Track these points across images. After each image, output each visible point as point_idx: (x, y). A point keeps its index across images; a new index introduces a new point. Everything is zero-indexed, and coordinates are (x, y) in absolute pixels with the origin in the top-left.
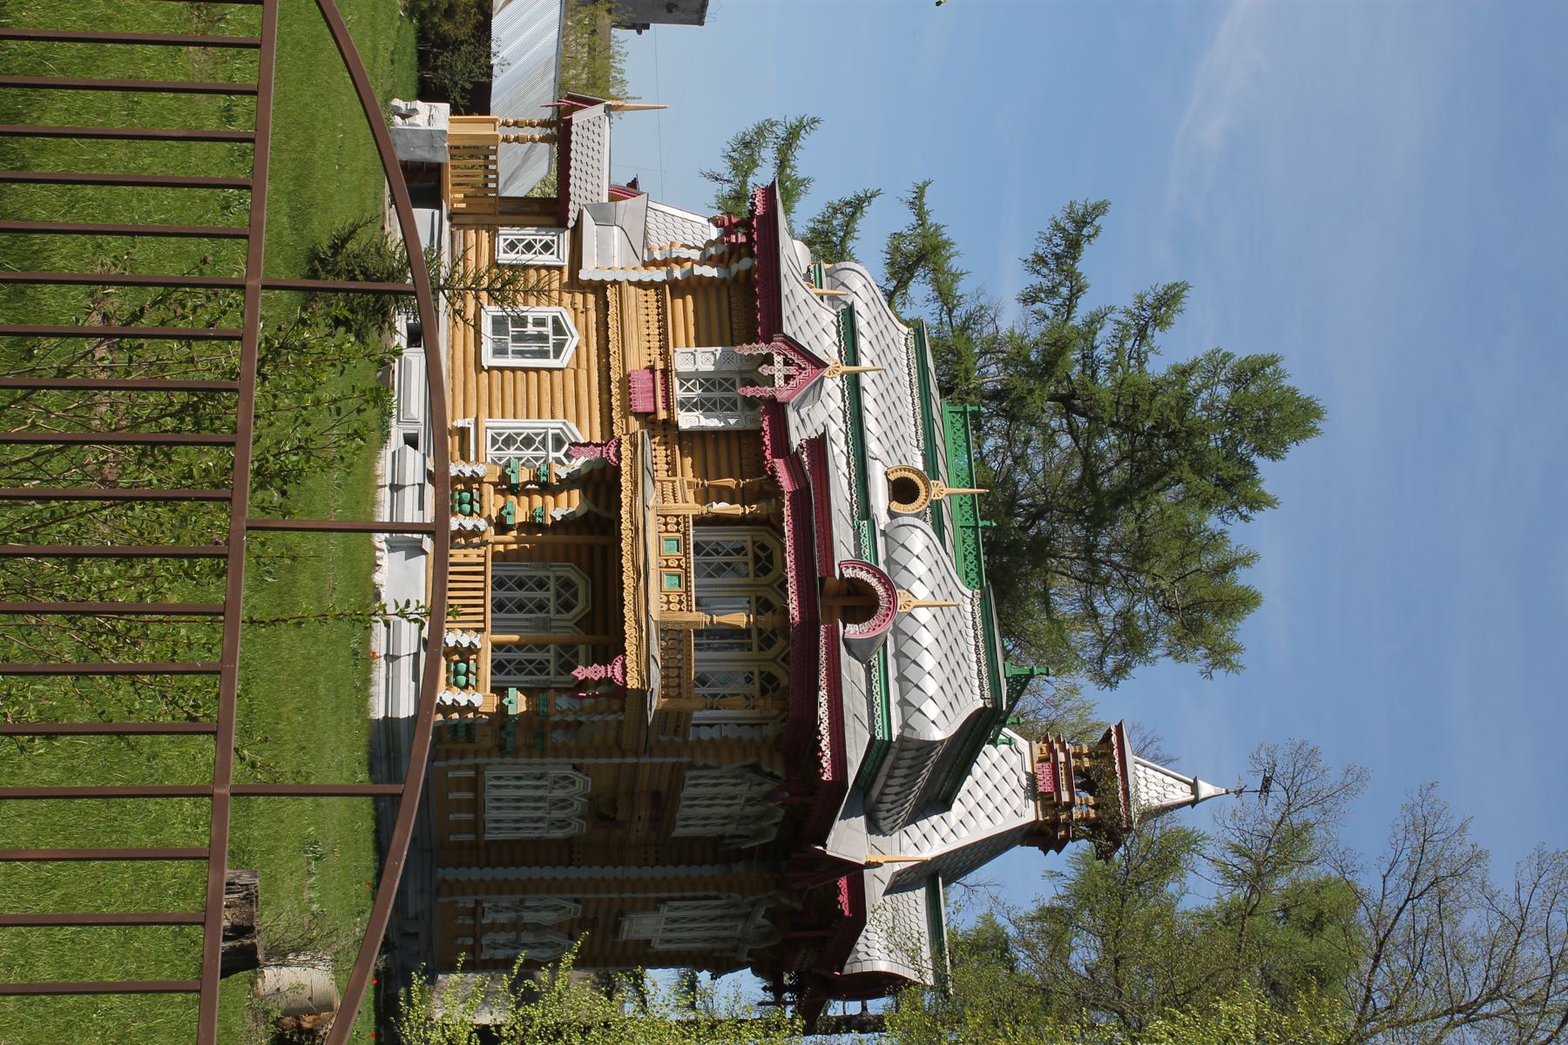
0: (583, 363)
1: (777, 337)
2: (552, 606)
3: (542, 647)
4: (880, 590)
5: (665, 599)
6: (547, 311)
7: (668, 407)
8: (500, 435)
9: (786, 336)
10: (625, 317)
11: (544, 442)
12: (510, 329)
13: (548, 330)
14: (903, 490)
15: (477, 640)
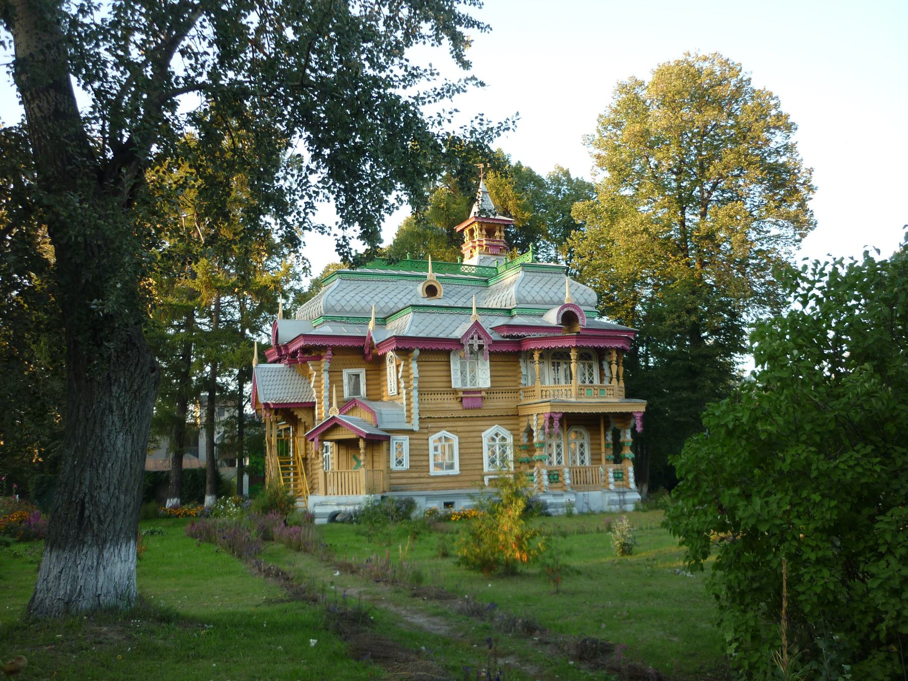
0: (455, 429)
1: (463, 342)
7: (480, 391)
13: (439, 445)
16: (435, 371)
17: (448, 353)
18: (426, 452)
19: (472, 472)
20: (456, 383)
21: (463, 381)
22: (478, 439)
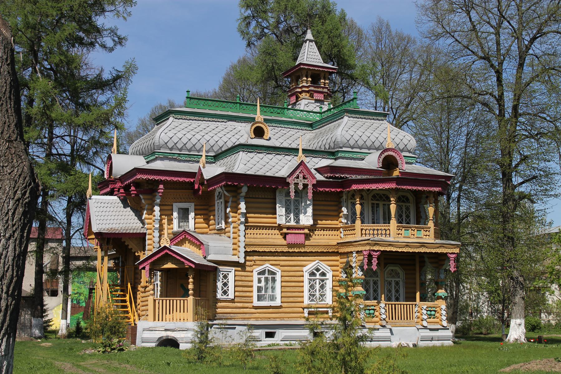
1: (289, 180)
2: (375, 279)
3: (390, 283)
6: (255, 277)
9: (288, 176)
10: (266, 243)
13: (263, 278)
17: (274, 191)
19: (293, 305)
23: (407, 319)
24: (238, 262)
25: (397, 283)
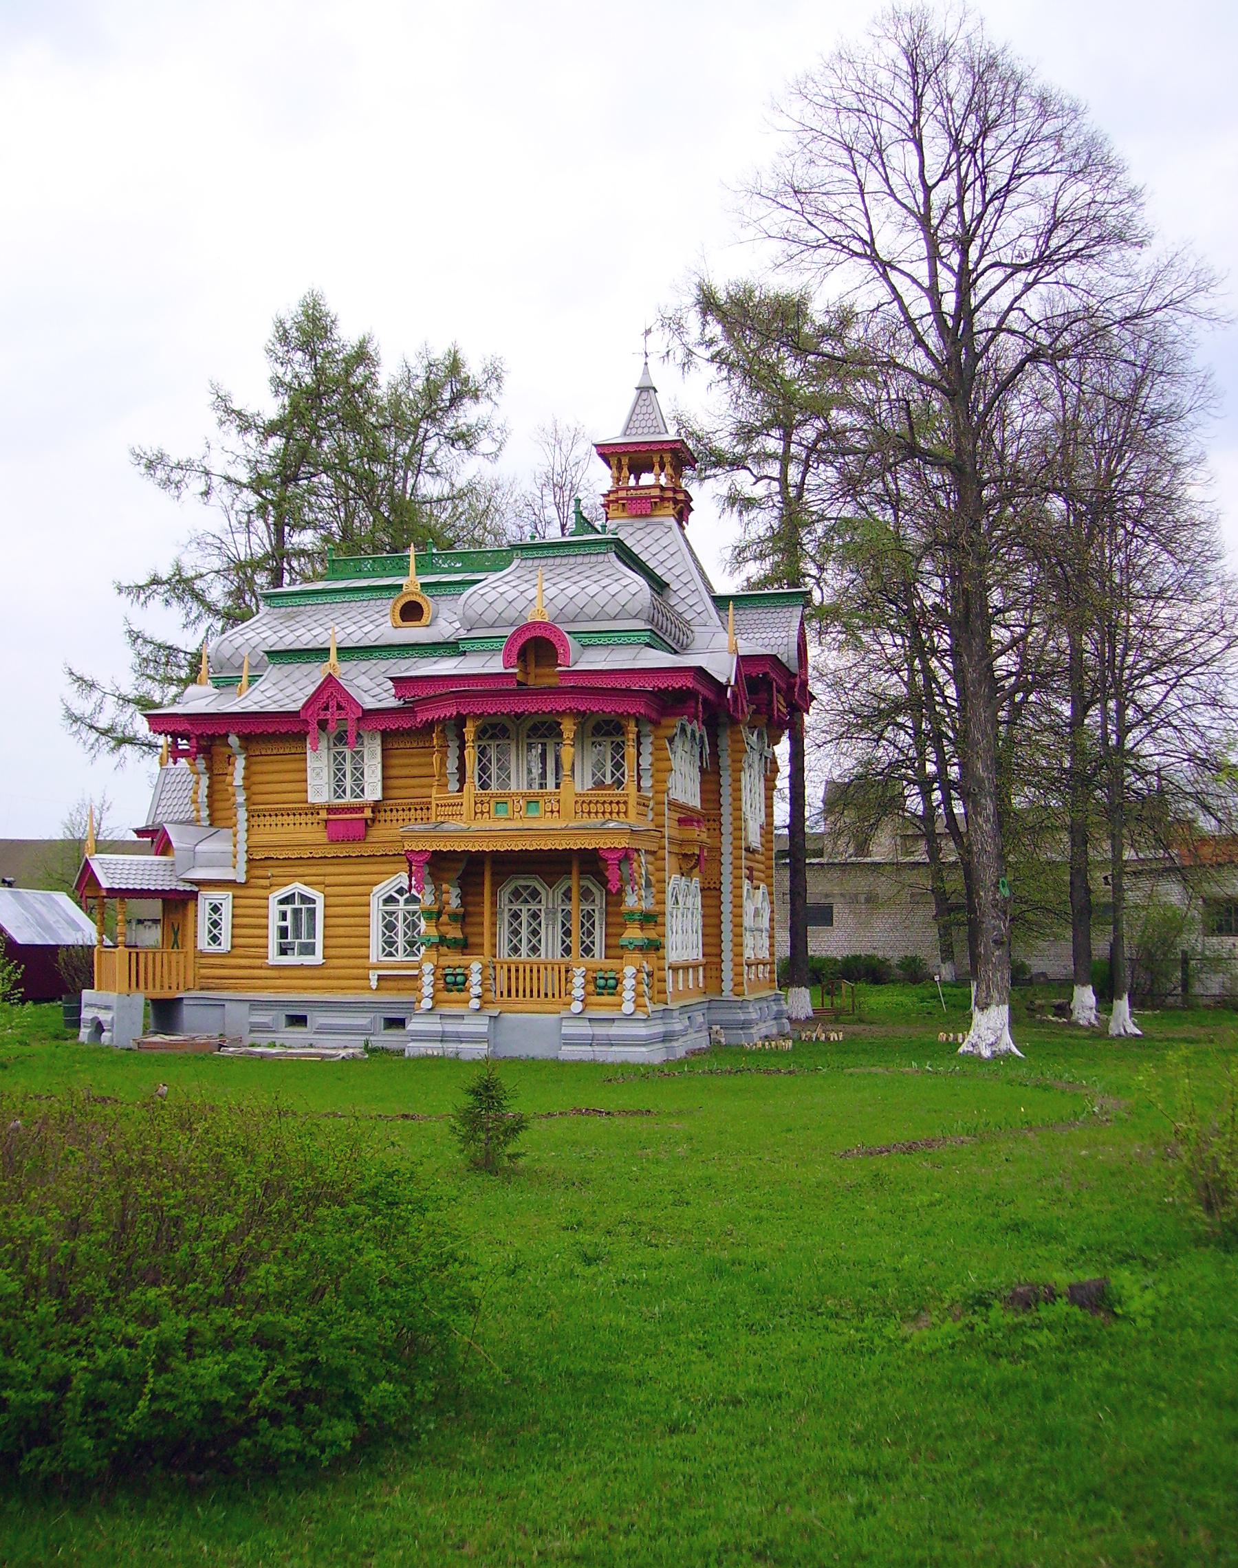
0: (320, 879)
2: (534, 907)
3: (567, 915)
4: (528, 635)
5: (549, 814)
6: (274, 909)
7: (360, 809)
8: (384, 950)
11: (391, 914)
12: (289, 940)
13: (288, 908)
14: (411, 612)
15: (579, 971)
16: (274, 769)
17: (301, 737)
18: (263, 921)
20: (318, 792)
21: (339, 789)
22: (363, 899)
23: (509, 995)
24: (234, 882)
25: (589, 915)
